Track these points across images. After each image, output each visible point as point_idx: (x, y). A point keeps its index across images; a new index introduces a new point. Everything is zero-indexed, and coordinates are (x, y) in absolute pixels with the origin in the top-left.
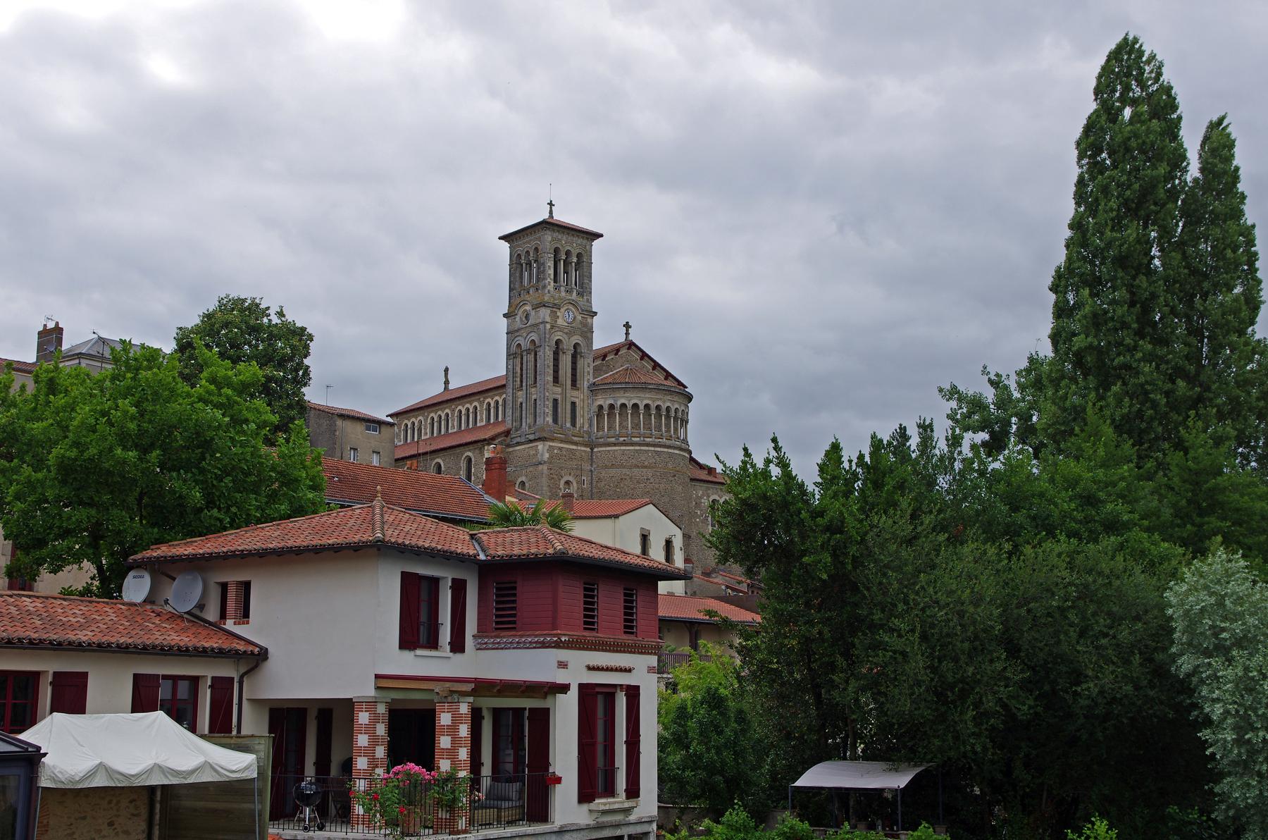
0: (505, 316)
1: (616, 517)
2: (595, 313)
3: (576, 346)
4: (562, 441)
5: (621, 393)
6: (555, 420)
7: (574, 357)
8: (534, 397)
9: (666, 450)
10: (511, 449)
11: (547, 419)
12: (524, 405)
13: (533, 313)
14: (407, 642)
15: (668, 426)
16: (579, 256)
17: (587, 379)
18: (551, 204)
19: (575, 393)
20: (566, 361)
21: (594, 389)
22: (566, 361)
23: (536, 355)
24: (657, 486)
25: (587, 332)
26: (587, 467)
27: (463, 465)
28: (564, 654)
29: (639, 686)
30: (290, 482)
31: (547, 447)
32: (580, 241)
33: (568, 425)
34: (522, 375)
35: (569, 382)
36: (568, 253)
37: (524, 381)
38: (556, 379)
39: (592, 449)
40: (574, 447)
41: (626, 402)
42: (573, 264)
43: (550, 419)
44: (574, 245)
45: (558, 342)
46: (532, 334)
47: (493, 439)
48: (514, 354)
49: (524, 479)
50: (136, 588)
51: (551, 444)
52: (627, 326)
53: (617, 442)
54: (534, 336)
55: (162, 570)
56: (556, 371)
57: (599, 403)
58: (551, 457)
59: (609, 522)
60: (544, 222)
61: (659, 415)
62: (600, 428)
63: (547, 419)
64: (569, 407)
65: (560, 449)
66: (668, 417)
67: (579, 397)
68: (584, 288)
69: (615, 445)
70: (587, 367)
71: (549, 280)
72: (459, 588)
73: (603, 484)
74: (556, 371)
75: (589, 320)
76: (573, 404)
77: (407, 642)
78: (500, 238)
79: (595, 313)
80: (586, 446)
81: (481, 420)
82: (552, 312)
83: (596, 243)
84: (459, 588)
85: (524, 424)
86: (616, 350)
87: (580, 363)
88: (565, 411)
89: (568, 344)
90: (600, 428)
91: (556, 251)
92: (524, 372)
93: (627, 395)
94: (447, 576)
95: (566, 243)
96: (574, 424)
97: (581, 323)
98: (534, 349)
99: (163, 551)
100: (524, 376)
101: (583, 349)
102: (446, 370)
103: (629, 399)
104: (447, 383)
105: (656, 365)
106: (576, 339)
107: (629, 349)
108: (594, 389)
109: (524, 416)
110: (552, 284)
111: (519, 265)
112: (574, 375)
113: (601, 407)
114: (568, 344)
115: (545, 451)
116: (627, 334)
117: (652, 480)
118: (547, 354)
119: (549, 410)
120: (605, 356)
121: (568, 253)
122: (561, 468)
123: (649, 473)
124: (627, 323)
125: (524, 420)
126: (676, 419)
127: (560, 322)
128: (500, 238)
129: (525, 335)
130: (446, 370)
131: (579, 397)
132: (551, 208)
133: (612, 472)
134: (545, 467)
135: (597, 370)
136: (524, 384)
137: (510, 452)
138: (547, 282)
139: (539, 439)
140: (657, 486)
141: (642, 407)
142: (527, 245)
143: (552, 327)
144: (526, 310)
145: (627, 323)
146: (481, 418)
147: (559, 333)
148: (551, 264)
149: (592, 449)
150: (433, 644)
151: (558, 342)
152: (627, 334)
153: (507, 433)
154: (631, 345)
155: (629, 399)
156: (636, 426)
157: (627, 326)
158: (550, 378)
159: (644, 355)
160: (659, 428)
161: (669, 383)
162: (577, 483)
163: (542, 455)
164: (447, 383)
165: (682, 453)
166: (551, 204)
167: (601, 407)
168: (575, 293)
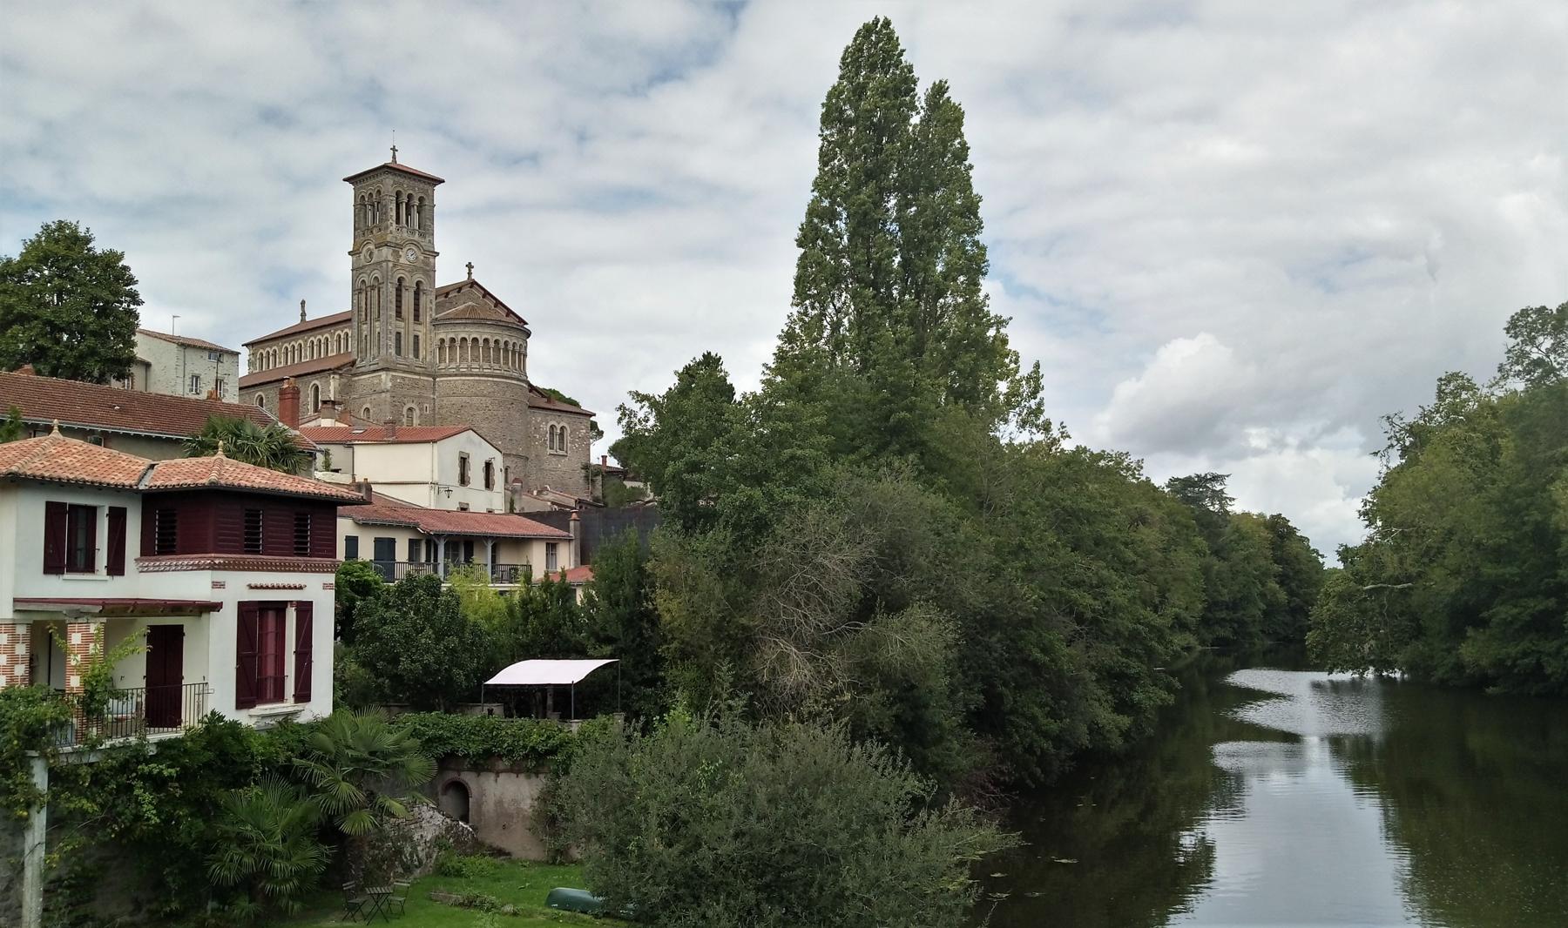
0: (349, 253)
1: (435, 442)
2: (438, 254)
3: (418, 284)
4: (405, 372)
5: (458, 329)
6: (398, 352)
7: (417, 294)
8: (378, 330)
9: (504, 380)
10: (356, 378)
11: (390, 351)
12: (368, 337)
13: (376, 251)
14: (53, 565)
15: (506, 358)
16: (421, 199)
17: (428, 313)
18: (394, 149)
19: (419, 327)
20: (408, 298)
22: (408, 298)
23: (379, 291)
24: (495, 413)
25: (430, 272)
28: (221, 576)
29: (239, 602)
31: (390, 377)
32: (421, 186)
33: (411, 356)
34: (366, 309)
35: (412, 318)
36: (410, 197)
37: (369, 315)
38: (399, 314)
39: (434, 379)
40: (417, 377)
41: (467, 337)
42: (416, 207)
43: (393, 351)
44: (416, 190)
45: (400, 280)
46: (376, 271)
49: (368, 406)
51: (394, 374)
52: (470, 266)
53: (457, 373)
54: (377, 274)
56: (399, 307)
57: (441, 336)
58: (394, 386)
59: (428, 447)
60: (385, 166)
61: (497, 349)
63: (390, 351)
64: (411, 339)
65: (403, 378)
66: (506, 350)
67: (421, 331)
68: (426, 229)
69: (456, 375)
70: (428, 302)
71: (391, 221)
72: (118, 520)
73: (444, 410)
74: (399, 307)
75: (431, 260)
76: (416, 337)
77: (53, 565)
78: (345, 180)
79: (438, 254)
80: (429, 376)
81: (332, 351)
82: (394, 251)
83: (438, 188)
84: (118, 518)
85: (368, 355)
86: (459, 288)
87: (423, 299)
88: (407, 343)
89: (410, 282)
91: (398, 194)
92: (369, 306)
93: (467, 329)
96: (417, 356)
97: (423, 262)
98: (377, 286)
100: (369, 311)
101: (424, 287)
102: (303, 303)
104: (303, 315)
105: (498, 303)
106: (418, 277)
107: (471, 287)
108: (436, 324)
109: (368, 347)
110: (394, 224)
111: (361, 205)
112: (417, 309)
113: (442, 341)
114: (410, 282)
115: (388, 380)
116: (470, 274)
117: (491, 407)
119: (392, 343)
120: (447, 294)
121: (410, 197)
122: (404, 396)
123: (489, 401)
124: (470, 263)
125: (368, 351)
126: (514, 352)
127: (402, 260)
128: (345, 180)
129: (369, 272)
130: (303, 303)
131: (421, 331)
132: (394, 153)
133: (454, 400)
135: (440, 307)
136: (368, 318)
137: (355, 381)
138: (389, 223)
139: (383, 369)
140: (495, 413)
141: (481, 341)
142: (370, 187)
143: (395, 266)
144: (369, 249)
145: (470, 263)
146: (332, 348)
147: (401, 271)
148: (393, 206)
149: (434, 379)
150: (90, 567)
151: (400, 280)
152: (470, 274)
153: (353, 363)
155: (470, 333)
158: (393, 313)
159: (486, 294)
161: (511, 319)
162: (421, 409)
163: (385, 384)
164: (303, 315)
165: (519, 383)
166: (394, 149)
167: (442, 341)
168: (417, 234)
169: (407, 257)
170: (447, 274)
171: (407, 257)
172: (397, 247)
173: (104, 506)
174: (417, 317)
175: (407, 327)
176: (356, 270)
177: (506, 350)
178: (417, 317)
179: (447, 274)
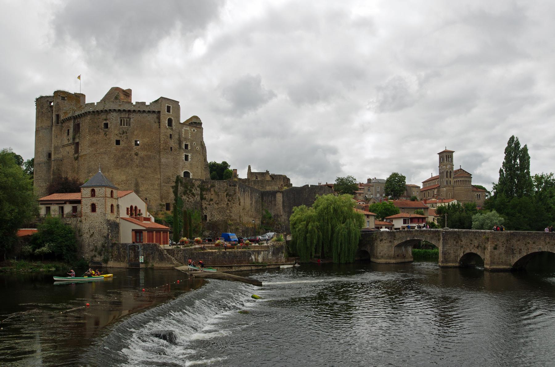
6: (447, 184)
14: (404, 224)
16: (451, 156)
17: (453, 176)
20: (449, 174)
21: (454, 178)
22: (449, 174)
25: (452, 168)
26: (452, 191)
27: (432, 192)
30: (396, 211)
36: (449, 156)
38: (447, 177)
47: (436, 188)
48: (440, 173)
50: (385, 220)
52: (460, 166)
54: (443, 170)
55: (387, 219)
61: (467, 181)
62: (455, 184)
67: (451, 180)
68: (452, 161)
77: (404, 224)
83: (454, 153)
86: (458, 170)
87: (451, 174)
90: (455, 184)
91: (446, 156)
94: (407, 219)
95: (448, 154)
96: (450, 184)
98: (443, 173)
99: (386, 218)
103: (460, 179)
108: (454, 178)
114: (449, 171)
118: (445, 173)
119: (446, 183)
121: (449, 156)
131: (451, 180)
134: (445, 192)
135: (454, 175)
146: (436, 182)
153: (439, 186)
154: (461, 169)
155: (460, 179)
156: (461, 183)
157: (460, 166)
159: (464, 171)
160: (465, 183)
169: (448, 167)
170: (456, 168)
171: (448, 167)
172: (446, 165)
173: (407, 219)
174: (450, 177)
175: (450, 179)
176: (440, 170)
177: (467, 181)
178: (450, 177)
179: (456, 168)
